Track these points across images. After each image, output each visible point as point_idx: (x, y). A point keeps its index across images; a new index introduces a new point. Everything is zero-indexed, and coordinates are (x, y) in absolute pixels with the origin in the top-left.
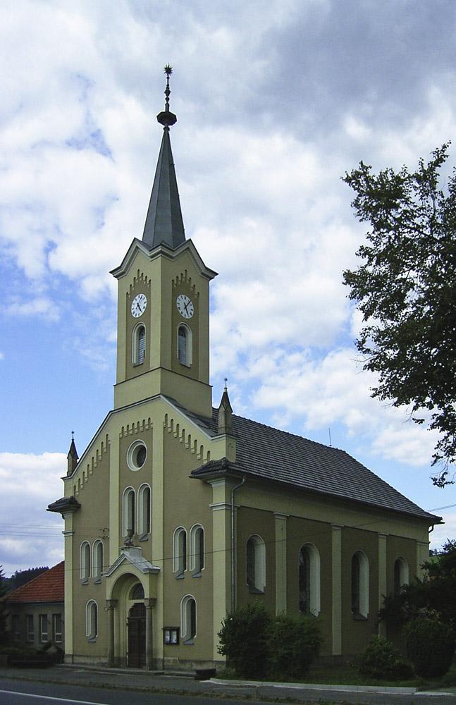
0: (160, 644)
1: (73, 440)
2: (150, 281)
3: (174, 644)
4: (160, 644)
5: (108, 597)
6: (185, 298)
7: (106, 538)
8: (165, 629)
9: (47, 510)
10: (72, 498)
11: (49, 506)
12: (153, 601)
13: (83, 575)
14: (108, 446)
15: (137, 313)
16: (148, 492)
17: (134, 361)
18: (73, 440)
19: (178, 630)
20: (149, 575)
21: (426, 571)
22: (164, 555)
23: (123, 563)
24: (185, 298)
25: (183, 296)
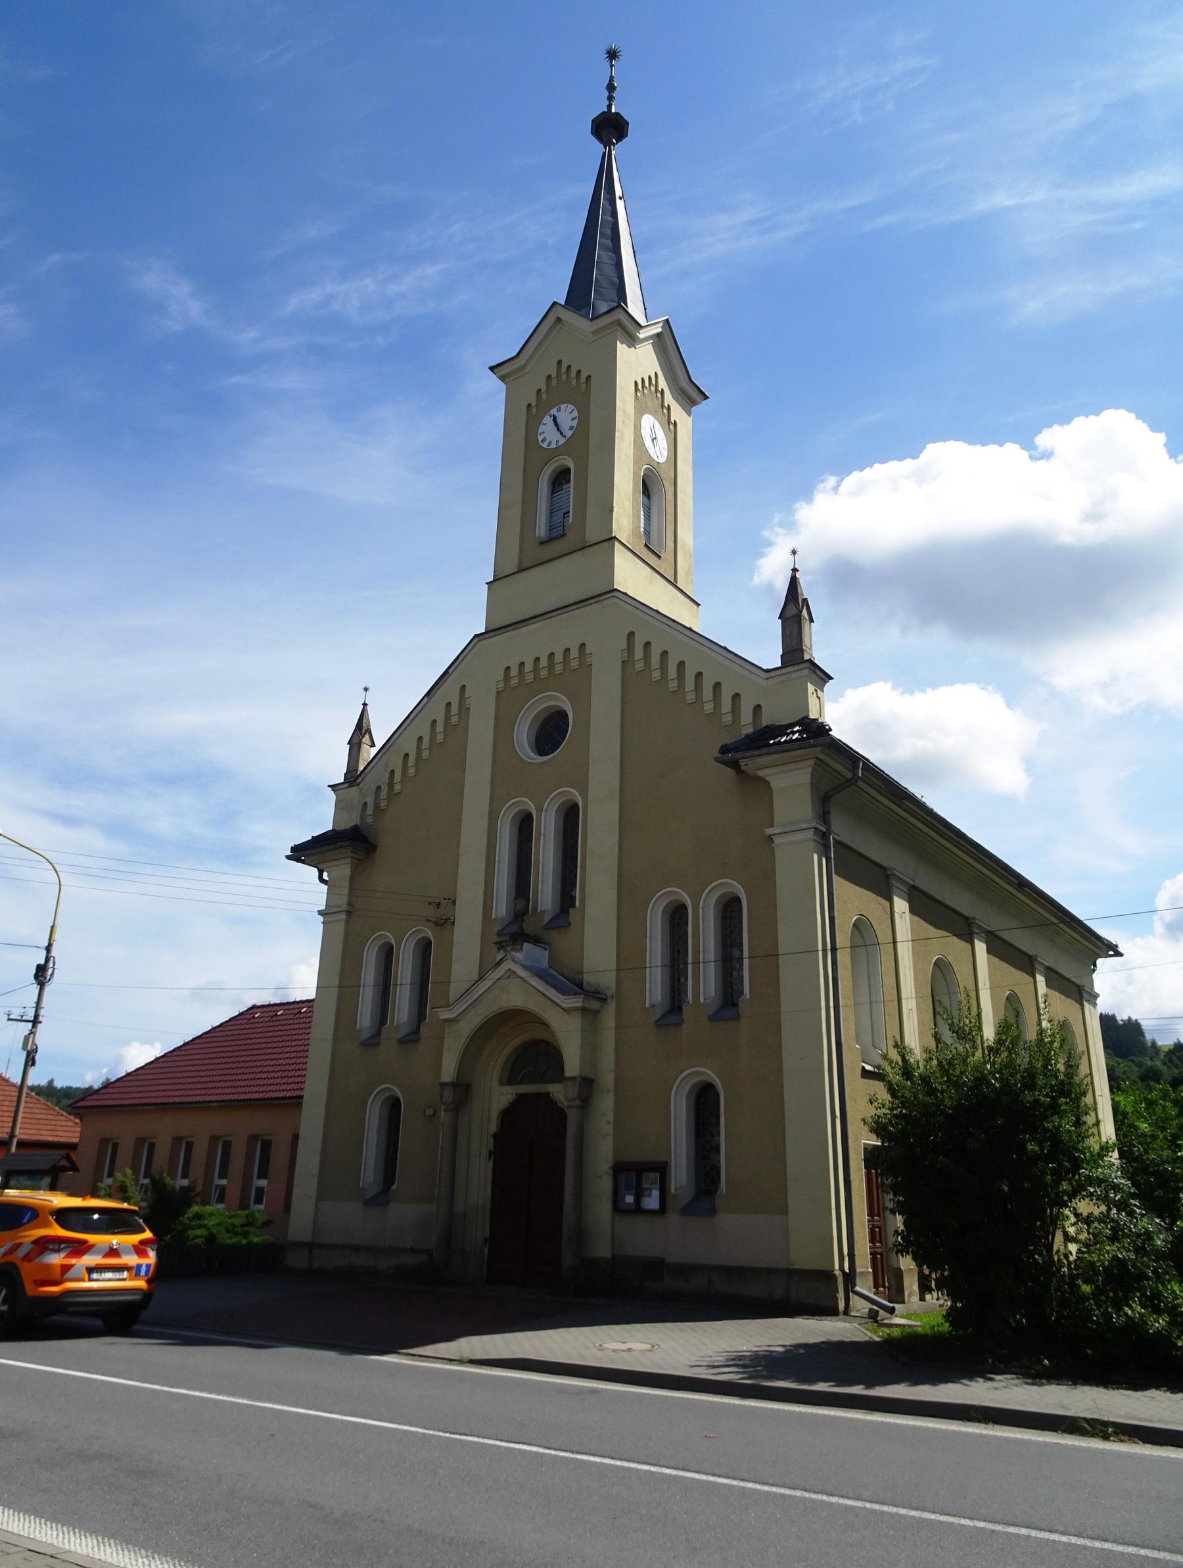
0: (601, 1210)
1: (365, 705)
2: (589, 377)
3: (652, 1212)
4: (601, 1210)
5: (448, 1070)
6: (573, 419)
7: (445, 923)
8: (619, 1169)
9: (288, 857)
10: (355, 829)
11: (294, 849)
12: (587, 1084)
13: (365, 1017)
14: (464, 710)
15: (548, 435)
16: (570, 816)
17: (541, 530)
18: (365, 705)
19: (662, 1169)
20: (579, 1013)
21: (928, 1297)
22: (618, 961)
23: (473, 983)
24: (573, 419)
25: (575, 414)
